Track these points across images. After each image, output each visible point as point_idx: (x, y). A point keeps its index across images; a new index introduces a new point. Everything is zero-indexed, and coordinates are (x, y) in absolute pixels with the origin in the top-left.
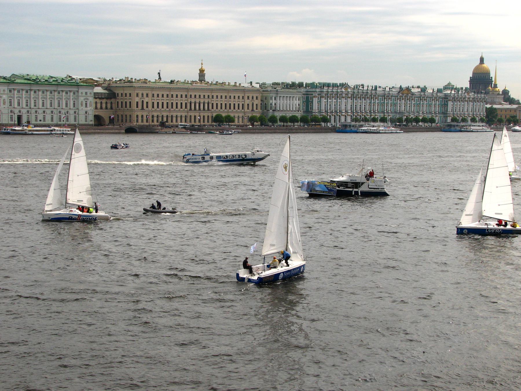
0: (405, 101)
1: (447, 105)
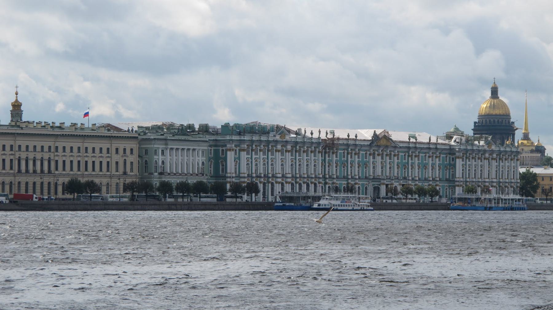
0: (382, 158)
1: (454, 166)
